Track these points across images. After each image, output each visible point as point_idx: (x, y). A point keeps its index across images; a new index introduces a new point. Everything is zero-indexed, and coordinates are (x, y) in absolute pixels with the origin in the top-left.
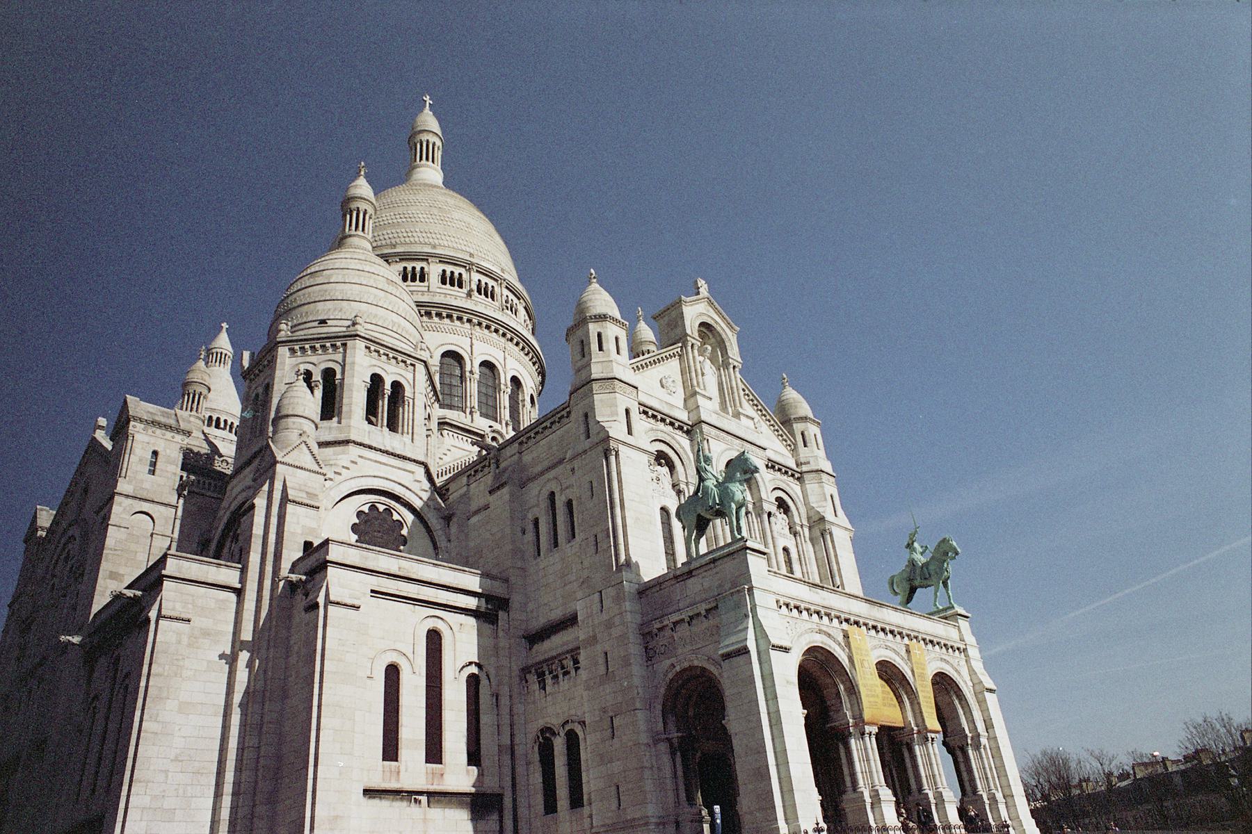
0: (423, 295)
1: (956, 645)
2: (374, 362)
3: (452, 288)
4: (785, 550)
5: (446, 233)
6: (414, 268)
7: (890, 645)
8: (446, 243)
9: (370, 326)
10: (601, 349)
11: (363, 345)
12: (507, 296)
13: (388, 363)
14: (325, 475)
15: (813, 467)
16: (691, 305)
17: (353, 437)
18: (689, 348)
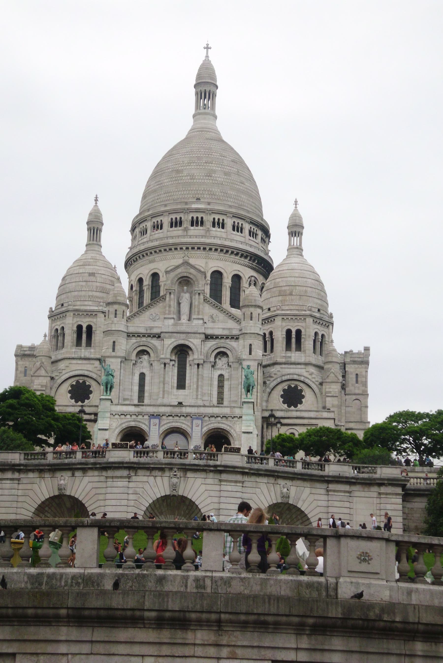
0: (157, 241)
1: (233, 416)
2: (78, 319)
3: (176, 229)
4: (221, 376)
5: (176, 190)
6: (158, 221)
8: (176, 197)
9: (78, 303)
10: (108, 318)
11: (72, 314)
12: (214, 219)
13: (85, 318)
14: (50, 377)
15: (243, 331)
16: (173, 272)
17: (68, 356)
18: (168, 296)
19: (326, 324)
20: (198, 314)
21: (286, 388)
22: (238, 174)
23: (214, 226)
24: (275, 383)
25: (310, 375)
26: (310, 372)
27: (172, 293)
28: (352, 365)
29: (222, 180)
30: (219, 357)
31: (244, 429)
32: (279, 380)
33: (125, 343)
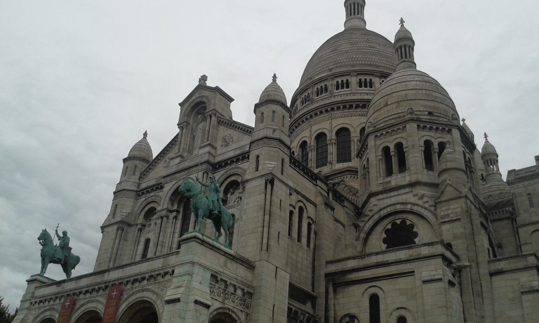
1: (162, 272)
7: (96, 299)
12: (337, 82)
16: (187, 102)
19: (443, 129)
20: (208, 140)
21: (389, 227)
22: (368, 41)
23: (338, 89)
24: (371, 223)
25: (419, 199)
26: (419, 196)
27: (184, 127)
28: (518, 184)
29: (348, 49)
30: (231, 190)
31: (169, 294)
32: (376, 217)
33: (131, 204)
